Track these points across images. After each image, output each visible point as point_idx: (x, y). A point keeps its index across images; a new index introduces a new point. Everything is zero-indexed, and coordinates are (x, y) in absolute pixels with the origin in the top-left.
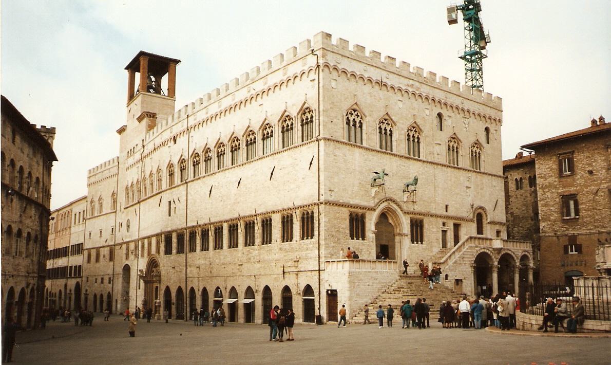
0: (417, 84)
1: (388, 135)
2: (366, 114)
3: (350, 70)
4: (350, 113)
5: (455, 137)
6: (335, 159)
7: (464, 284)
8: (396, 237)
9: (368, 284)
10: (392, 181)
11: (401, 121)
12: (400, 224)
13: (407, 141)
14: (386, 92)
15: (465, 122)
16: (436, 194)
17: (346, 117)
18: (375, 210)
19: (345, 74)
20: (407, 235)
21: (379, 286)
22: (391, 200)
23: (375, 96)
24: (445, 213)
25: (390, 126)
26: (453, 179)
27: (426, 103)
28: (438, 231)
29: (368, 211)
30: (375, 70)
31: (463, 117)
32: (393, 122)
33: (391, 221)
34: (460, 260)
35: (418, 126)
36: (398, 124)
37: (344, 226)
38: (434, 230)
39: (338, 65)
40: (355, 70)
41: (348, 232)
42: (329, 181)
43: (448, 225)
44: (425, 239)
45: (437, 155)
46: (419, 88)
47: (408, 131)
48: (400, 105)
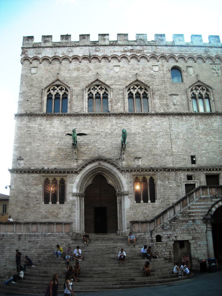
0: (138, 48)
3: (50, 56)
4: (52, 90)
5: (203, 85)
6: (28, 131)
7: (192, 246)
8: (118, 198)
9: (24, 248)
10: (104, 140)
11: (119, 83)
12: (118, 182)
13: (127, 100)
14: (98, 63)
15: (215, 68)
16: (174, 146)
17: (48, 93)
18: (77, 173)
19: (47, 60)
20: (127, 195)
21: (41, 251)
22: (101, 160)
24: (190, 165)
26: (201, 127)
27: (153, 62)
28: (178, 186)
29: (69, 175)
30: (82, 49)
31: (211, 64)
33: (110, 182)
34: (182, 216)
35: (142, 83)
37: (35, 192)
38: (171, 186)
39: (38, 56)
40: (57, 55)
41: (41, 197)
42: (20, 151)
43: (197, 178)
44: (158, 196)
45: (173, 106)
46: (142, 51)
47: (129, 89)
48: (117, 69)
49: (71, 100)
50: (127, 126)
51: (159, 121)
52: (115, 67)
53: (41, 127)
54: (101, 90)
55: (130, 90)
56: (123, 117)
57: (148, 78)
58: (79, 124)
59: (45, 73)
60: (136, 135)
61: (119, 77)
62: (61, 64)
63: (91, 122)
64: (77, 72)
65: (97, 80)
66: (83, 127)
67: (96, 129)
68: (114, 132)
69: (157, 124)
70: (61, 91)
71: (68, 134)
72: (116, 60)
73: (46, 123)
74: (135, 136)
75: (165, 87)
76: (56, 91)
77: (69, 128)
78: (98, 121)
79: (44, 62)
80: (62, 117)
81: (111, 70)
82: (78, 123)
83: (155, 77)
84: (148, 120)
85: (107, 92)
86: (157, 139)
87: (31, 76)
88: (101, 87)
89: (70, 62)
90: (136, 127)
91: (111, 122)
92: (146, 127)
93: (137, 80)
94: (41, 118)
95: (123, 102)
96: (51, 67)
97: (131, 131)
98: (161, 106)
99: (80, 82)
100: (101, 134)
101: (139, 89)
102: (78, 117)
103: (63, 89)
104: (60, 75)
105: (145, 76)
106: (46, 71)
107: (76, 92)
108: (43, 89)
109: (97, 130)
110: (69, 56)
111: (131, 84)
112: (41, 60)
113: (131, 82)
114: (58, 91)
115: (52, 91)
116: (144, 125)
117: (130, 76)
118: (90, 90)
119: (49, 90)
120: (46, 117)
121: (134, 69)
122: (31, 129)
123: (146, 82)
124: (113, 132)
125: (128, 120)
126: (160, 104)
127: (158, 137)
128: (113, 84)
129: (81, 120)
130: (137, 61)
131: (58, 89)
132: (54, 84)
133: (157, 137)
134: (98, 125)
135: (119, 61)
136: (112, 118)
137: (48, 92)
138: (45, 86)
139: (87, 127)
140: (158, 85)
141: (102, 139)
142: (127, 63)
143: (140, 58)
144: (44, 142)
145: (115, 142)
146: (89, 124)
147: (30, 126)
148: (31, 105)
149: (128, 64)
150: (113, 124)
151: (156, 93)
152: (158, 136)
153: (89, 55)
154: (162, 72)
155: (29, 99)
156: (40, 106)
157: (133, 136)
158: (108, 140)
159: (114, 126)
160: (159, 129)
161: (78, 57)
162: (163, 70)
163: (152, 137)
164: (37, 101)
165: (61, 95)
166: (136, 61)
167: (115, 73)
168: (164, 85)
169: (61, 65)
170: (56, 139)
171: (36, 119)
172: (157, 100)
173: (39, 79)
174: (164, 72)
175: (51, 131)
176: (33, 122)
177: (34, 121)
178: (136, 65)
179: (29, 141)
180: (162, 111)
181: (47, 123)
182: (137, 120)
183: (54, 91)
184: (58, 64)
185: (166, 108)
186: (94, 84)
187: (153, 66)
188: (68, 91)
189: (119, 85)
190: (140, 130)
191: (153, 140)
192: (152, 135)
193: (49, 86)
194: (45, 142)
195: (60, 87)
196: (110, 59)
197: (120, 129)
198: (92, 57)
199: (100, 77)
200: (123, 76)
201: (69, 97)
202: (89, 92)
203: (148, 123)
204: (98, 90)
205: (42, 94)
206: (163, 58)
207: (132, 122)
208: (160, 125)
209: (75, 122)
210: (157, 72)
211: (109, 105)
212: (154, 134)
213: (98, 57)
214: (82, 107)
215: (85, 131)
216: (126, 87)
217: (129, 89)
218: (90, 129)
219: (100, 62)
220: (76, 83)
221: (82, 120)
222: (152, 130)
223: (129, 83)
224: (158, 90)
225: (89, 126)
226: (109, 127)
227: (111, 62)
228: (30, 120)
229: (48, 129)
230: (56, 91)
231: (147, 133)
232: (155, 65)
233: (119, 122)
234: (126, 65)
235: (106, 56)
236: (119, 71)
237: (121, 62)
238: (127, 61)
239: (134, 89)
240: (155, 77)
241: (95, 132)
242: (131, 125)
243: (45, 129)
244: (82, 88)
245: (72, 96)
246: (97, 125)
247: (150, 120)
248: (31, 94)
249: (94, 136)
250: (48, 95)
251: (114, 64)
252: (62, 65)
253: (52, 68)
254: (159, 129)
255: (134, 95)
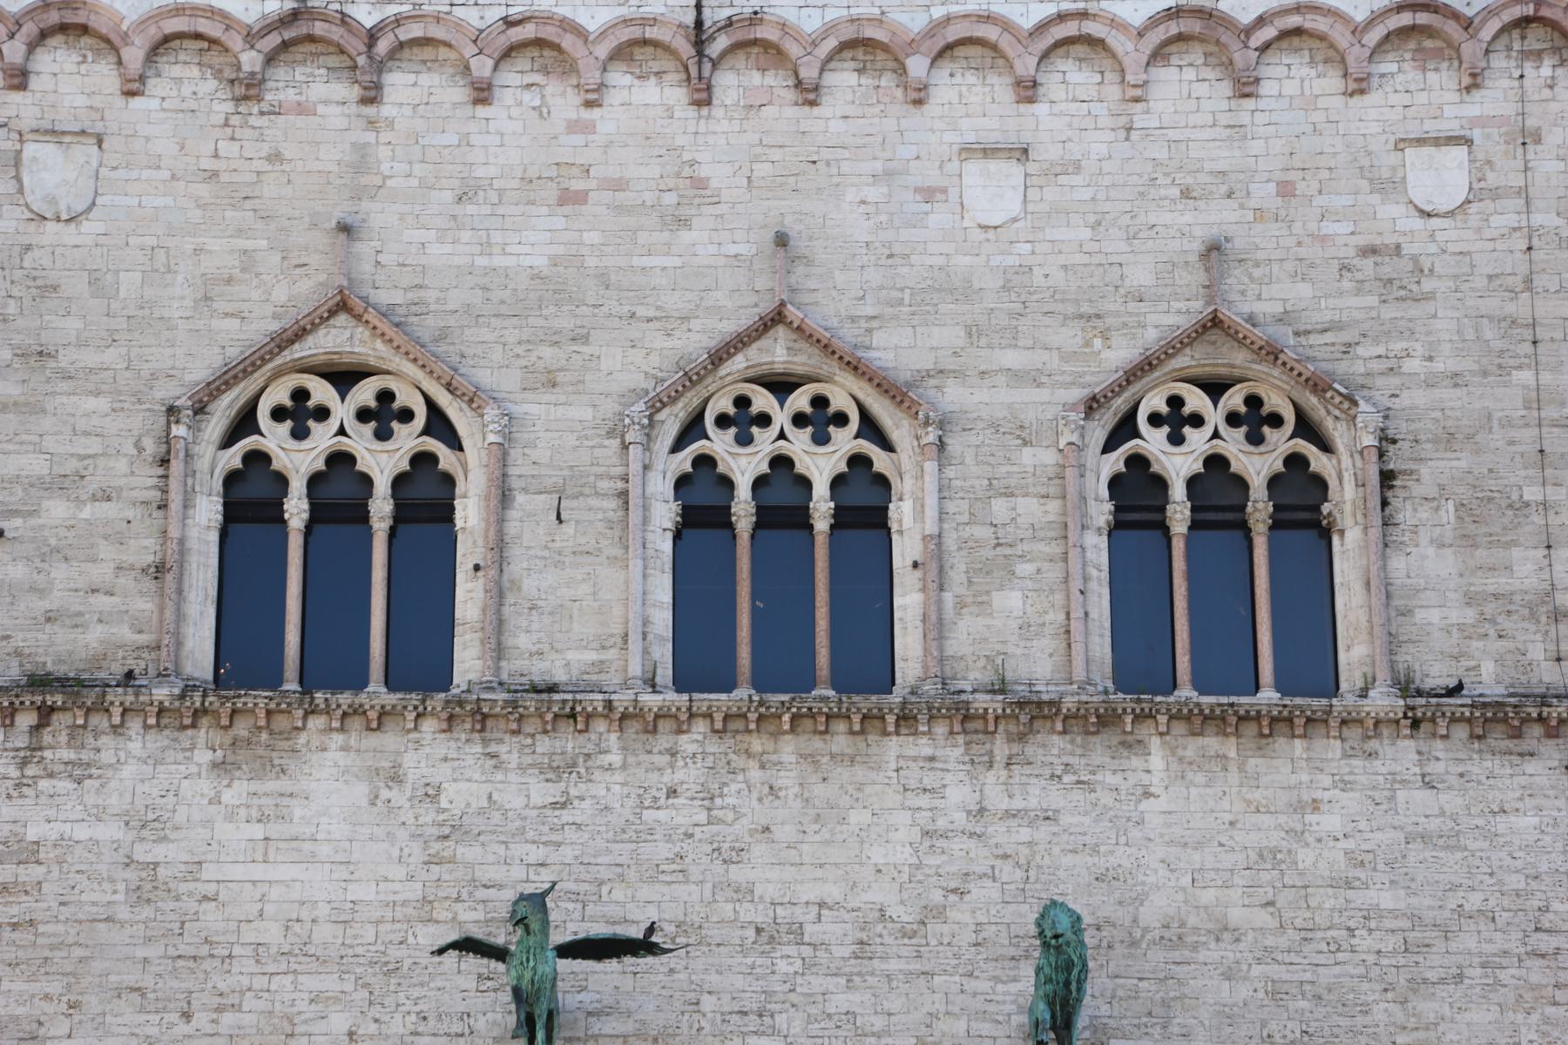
1: (822, 524)
2: (484, 377)
4: (278, 414)
10: (841, 1001)
11: (1012, 359)
13: (1097, 548)
14: (784, 114)
17: (233, 458)
23: (618, 185)
25: (845, 441)
32: (896, 393)
35: (1272, 353)
36: (953, 396)
47: (1125, 428)
49: (499, 546)
50: (1095, 850)
51: (1451, 801)
52: (973, 168)
53: (159, 852)
54: (821, 439)
55: (1136, 434)
56: (1052, 747)
57: (1341, 293)
58: (582, 812)
59: (196, 215)
60: (1195, 947)
61: (1015, 281)
62: (370, 110)
63: (709, 798)
64: (560, 222)
65: (777, 318)
66: (623, 852)
67: (760, 871)
68: (953, 915)
69: (1434, 825)
70: (383, 435)
71: (468, 945)
72: (993, 79)
73: (216, 800)
74: (1177, 955)
75: (1536, 399)
76: (322, 438)
77: (470, 866)
78: (787, 780)
79: (177, 71)
80: (390, 739)
81: (929, 194)
82: (563, 806)
83: (1428, 285)
84: (1326, 781)
85: (881, 461)
86: (1428, 1009)
87: (28, 248)
88: (820, 402)
89: (482, 94)
90: (1197, 857)
91: (924, 801)
92: (1305, 857)
93: (1214, 323)
94: (156, 741)
95: (1054, 573)
96: (265, 149)
97: (1140, 900)
98: (1483, 619)
99: (585, 339)
100: (808, 929)
101: (1233, 419)
102: (567, 742)
103: (406, 415)
104: (363, 248)
105: (1303, 271)
106: (203, 190)
107: (541, 454)
108: (172, 410)
109: (771, 892)
110: (459, 26)
111: (1145, 367)
112: (134, 55)
113: (1151, 337)
114: (342, 431)
115: (273, 438)
116: (1276, 839)
117: (1141, 275)
118: (692, 429)
119: (244, 423)
120: (218, 737)
121: (1186, 194)
122: (41, 870)
123: (1315, 339)
124: (939, 912)
125: (1111, 779)
126: (1470, 600)
127: (1442, 981)
128: (949, 363)
129: (597, 775)
130: (1226, 88)
131: (343, 411)
132: (299, 351)
133: (1425, 981)
134: (784, 833)
135: (1028, 90)
136: (932, 759)
137: (229, 441)
138: (200, 371)
139: (663, 851)
140: (1456, 380)
141: (817, 983)
142: (1105, 121)
143: (1265, 48)
144: (187, 1016)
145: (961, 1026)
146: (685, 813)
147: (32, 834)
148: (41, 592)
149: (1123, 120)
150: (941, 823)
151: (1424, 471)
152: (1434, 965)
153: (689, 18)
154: (1512, 220)
155: (18, 522)
156: (145, 605)
157: (1157, 956)
158: (887, 1005)
159: (958, 845)
160: (1454, 888)
161: (568, 41)
162: (1524, 193)
163: (1365, 977)
164: (106, 551)
165: (382, 486)
166: (1215, 93)
167: (979, 235)
168: (1526, 376)
169: (371, 123)
170: (330, 983)
171: (107, 756)
172: (1431, 551)
173: (129, 283)
174: (1537, 219)
175: (275, 893)
176: (64, 785)
177: (80, 772)
178: (1208, 133)
179: (20, 1011)
180: (1489, 680)
181: (228, 796)
182: (1200, 778)
183: (300, 434)
184: (335, 117)
185: (1537, 652)
186: (738, 363)
187: (1400, 145)
188: (455, 443)
189: (1018, 377)
190: (1235, 894)
191: (1379, 1013)
192: (1371, 959)
193: (246, 373)
194: (201, 1020)
195: (365, 393)
196: (917, 66)
197: (1019, 874)
198: (721, 43)
199: (811, 284)
200: (1058, 278)
201: (469, 513)
202: (683, 461)
203: (1330, 822)
204: (782, 436)
205: (164, 462)
206: (1536, 38)
207: (1146, 805)
208: (1458, 848)
209: (542, 792)
210: (1450, 214)
211: (897, 602)
212: (1392, 942)
213: (794, 50)
214: (617, 629)
215: (645, 892)
216: (1092, 406)
217: (1125, 428)
218: (695, 873)
219: (813, 103)
220: (547, 352)
221: (609, 768)
222: (1371, 897)
223: (1121, 354)
224: (1449, 440)
225: (687, 846)
226: (904, 855)
227: (931, 109)
228: (31, 771)
229: (238, 872)
230: (322, 438)
231: (1307, 933)
232: (1432, 128)
233: (1006, 804)
234: (1098, 144)
235: (879, 35)
236: (1015, 207)
237: (1041, 109)
238: (1113, 91)
239: (1177, 420)
240: (1428, 285)
241: (748, 913)
242: (1135, 834)
243: (209, 872)
244: (610, 407)
245: (503, 496)
246: (767, 829)
247: (1345, 786)
248: (37, 466)
249: (743, 950)
250: (231, 479)
251: (965, 123)
252: (390, 123)
253: (275, 157)
254: (1454, 888)
255: (1178, 491)
